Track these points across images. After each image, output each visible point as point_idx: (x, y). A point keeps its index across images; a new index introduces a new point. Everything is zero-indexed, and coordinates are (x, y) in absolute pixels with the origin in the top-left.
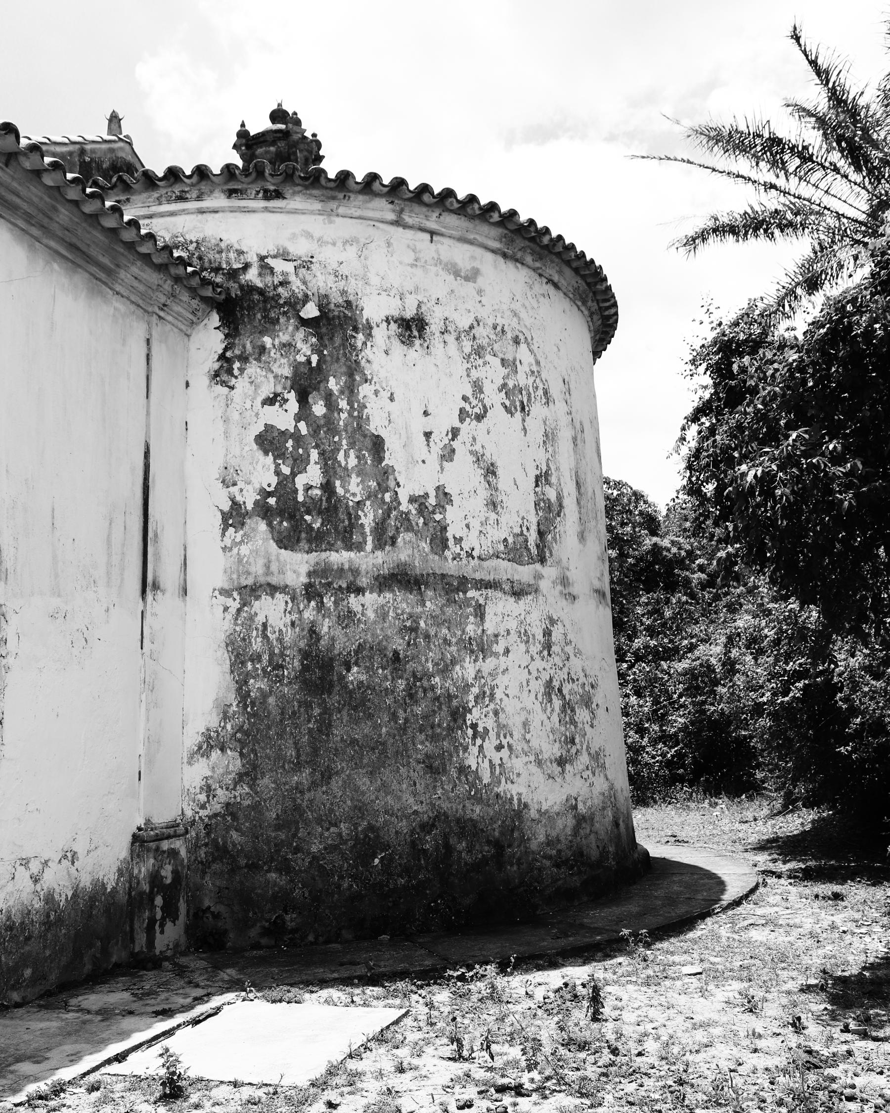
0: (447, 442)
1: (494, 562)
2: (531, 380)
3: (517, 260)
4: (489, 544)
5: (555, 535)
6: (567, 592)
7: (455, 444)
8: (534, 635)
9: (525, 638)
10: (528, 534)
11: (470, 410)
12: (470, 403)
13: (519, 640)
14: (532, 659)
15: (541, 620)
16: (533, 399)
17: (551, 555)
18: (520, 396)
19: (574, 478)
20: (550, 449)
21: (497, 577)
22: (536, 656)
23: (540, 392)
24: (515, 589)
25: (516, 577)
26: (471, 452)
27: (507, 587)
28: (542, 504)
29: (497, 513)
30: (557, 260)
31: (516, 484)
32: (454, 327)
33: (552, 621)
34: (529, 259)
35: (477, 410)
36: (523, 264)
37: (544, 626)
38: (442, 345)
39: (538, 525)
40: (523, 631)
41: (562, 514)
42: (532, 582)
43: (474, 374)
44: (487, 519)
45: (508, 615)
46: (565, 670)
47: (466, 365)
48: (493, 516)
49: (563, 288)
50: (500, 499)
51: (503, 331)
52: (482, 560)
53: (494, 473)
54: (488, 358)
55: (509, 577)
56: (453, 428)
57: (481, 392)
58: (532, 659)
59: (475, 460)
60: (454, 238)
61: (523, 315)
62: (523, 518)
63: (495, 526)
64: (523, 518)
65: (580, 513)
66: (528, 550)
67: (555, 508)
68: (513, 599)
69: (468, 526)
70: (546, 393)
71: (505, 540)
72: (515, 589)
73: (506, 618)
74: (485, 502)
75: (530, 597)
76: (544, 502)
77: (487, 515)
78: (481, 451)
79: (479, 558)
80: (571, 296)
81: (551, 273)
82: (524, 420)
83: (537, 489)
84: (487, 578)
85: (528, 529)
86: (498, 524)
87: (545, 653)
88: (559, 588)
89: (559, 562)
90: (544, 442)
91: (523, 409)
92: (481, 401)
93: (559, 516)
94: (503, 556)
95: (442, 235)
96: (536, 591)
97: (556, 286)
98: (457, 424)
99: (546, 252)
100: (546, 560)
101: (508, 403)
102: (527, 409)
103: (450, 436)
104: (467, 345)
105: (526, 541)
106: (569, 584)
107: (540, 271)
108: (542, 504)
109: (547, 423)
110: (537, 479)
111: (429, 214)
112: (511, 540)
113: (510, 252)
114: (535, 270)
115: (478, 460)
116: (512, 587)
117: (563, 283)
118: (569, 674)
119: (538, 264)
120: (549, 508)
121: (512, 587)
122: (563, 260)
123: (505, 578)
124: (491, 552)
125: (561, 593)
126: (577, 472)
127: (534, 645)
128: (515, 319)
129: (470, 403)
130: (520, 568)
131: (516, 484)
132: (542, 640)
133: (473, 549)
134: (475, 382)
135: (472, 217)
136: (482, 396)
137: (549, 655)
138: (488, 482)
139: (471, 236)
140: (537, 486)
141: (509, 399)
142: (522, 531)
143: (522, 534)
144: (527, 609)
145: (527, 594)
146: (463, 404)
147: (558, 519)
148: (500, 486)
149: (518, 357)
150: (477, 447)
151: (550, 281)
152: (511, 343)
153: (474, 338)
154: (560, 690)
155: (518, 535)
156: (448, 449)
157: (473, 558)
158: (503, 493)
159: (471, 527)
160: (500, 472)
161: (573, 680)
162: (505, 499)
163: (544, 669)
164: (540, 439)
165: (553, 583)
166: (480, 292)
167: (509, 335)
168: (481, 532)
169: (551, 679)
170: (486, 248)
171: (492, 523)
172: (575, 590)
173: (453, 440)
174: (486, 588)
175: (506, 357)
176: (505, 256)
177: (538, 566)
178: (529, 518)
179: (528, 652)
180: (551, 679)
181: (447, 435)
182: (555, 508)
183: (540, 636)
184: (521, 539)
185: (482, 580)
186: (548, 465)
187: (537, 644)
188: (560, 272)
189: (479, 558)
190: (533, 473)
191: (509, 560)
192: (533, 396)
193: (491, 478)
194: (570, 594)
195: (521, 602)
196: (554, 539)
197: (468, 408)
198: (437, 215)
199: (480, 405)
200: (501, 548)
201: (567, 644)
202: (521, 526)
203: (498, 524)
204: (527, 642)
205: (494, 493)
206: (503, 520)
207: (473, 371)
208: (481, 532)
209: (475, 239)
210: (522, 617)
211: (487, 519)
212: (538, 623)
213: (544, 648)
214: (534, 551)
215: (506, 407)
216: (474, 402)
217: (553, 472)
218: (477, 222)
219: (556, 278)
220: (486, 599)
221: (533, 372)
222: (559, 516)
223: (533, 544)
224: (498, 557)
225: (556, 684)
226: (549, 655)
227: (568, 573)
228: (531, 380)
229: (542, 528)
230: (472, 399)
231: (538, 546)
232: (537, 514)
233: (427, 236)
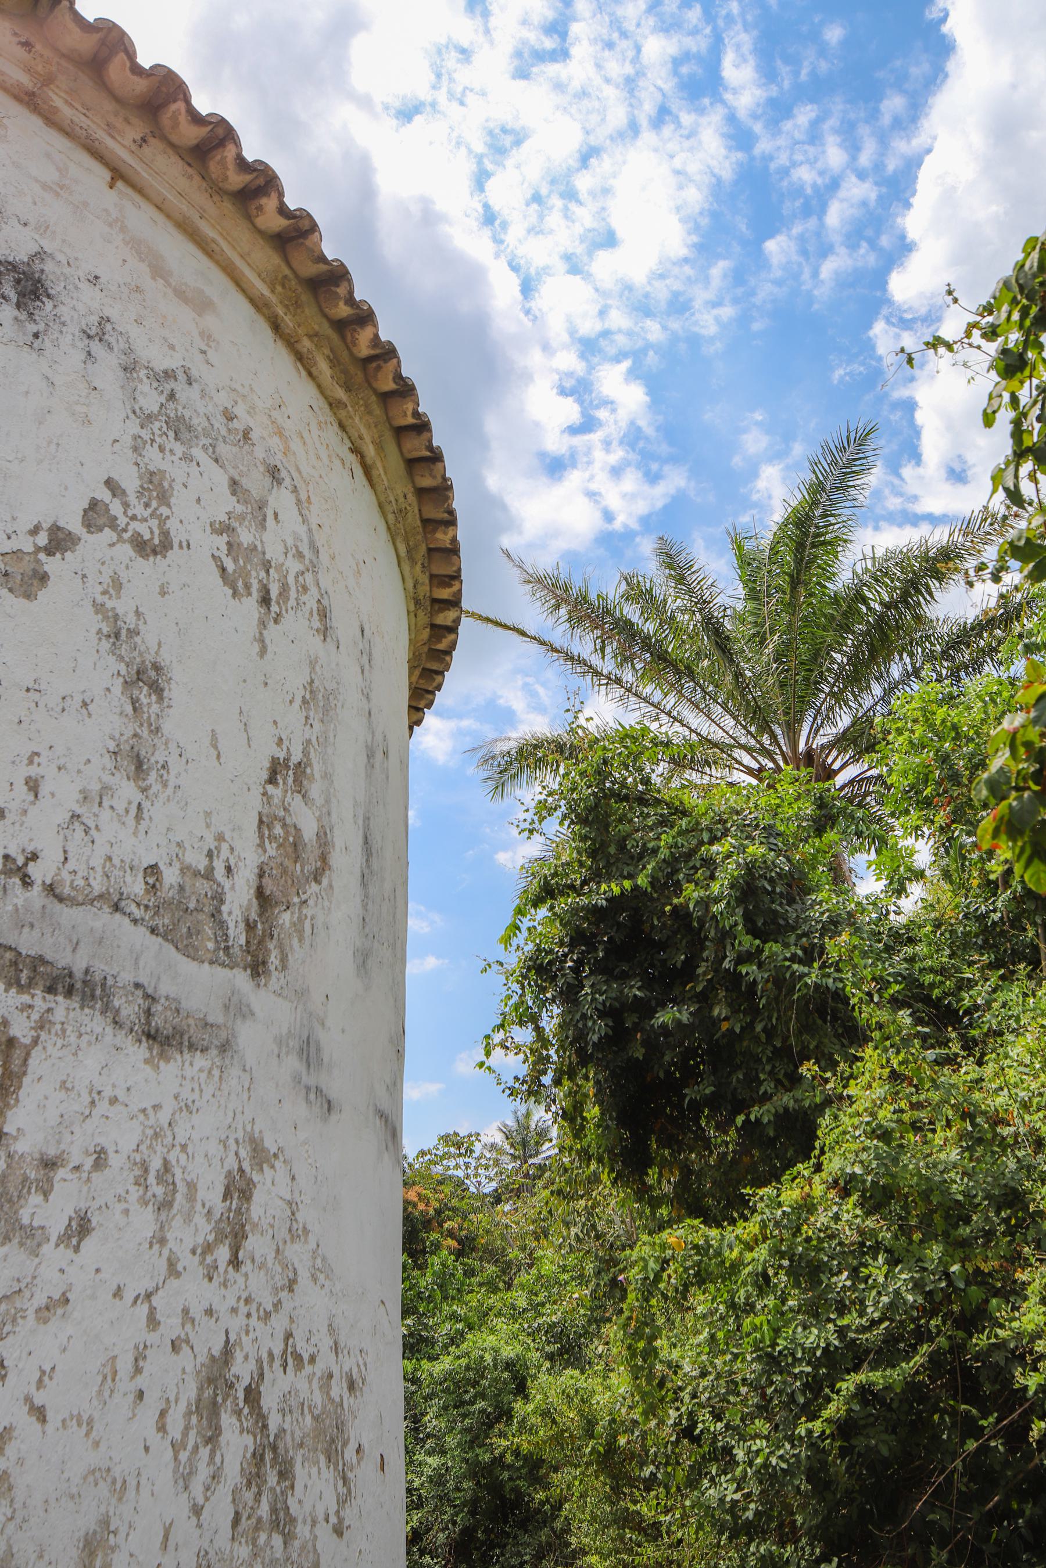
0: (29, 548)
1: (102, 919)
2: (294, 566)
3: (299, 357)
4: (97, 862)
5: (301, 920)
6: (312, 1081)
7: (51, 565)
8: (192, 1186)
9: (159, 1190)
10: (227, 884)
11: (122, 521)
12: (126, 505)
13: (135, 1193)
14: (173, 1269)
15: (224, 1142)
16: (292, 603)
17: (284, 966)
18: (263, 574)
19: (360, 822)
20: (317, 725)
21: (100, 968)
22: (187, 1261)
23: (310, 600)
24: (157, 1021)
25: (166, 988)
26: (99, 608)
27: (129, 1009)
28: (278, 830)
29: (144, 790)
30: (378, 411)
31: (216, 747)
32: (122, 345)
33: (261, 1156)
34: (323, 367)
35: (143, 529)
36: (310, 374)
37: (231, 1163)
38: (83, 356)
39: (261, 876)
40: (156, 1164)
41: (325, 881)
42: (216, 1017)
43: (153, 457)
44: (105, 790)
45: (113, 1101)
46: (279, 1323)
47: (133, 427)
48: (127, 791)
49: (380, 488)
50: (160, 757)
51: (246, 435)
52: (61, 899)
53: (157, 689)
54: (197, 452)
55: (143, 980)
56: (55, 529)
57: (164, 498)
58: (173, 1269)
59: (105, 630)
60: (168, 216)
61: (296, 445)
62: (220, 838)
63: (130, 820)
64: (220, 838)
65: (365, 907)
66: (222, 925)
67: (312, 863)
68: (138, 1052)
69: (33, 786)
70: (323, 614)
71: (153, 870)
72: (157, 1021)
73: (103, 1107)
74: (112, 745)
75: (201, 1061)
76: (284, 826)
77: (107, 778)
78: (131, 620)
79: (50, 889)
80: (391, 517)
81: (364, 431)
82: (263, 624)
83: (270, 788)
84: (63, 959)
85: (229, 869)
86: (139, 817)
87: (223, 1253)
88: (293, 1063)
89: (302, 994)
90: (305, 701)
91: (265, 600)
92: (163, 521)
93: (318, 881)
94: (138, 913)
95: (140, 190)
96: (224, 1048)
97: (367, 470)
98: (74, 524)
99: (360, 376)
100: (267, 973)
101: (230, 566)
102: (274, 608)
103: (42, 539)
104: (151, 400)
105: (219, 898)
106: (320, 1062)
107: (342, 413)
108: (278, 830)
109: (317, 668)
110: (275, 771)
111: (119, 123)
112: (171, 876)
113: (288, 321)
114: (334, 405)
115: (117, 635)
116: (148, 1013)
117: (379, 471)
118: (289, 1336)
119: (340, 394)
120: (295, 847)
121: (148, 1013)
122: (388, 419)
123: (127, 977)
124: (98, 886)
125: (297, 1080)
126: (367, 819)
127: (188, 1219)
128: (276, 439)
129: (126, 505)
130: (186, 966)
131: (216, 747)
132: (220, 1208)
133: (34, 857)
134: (152, 474)
135: (217, 189)
136: (164, 511)
137: (235, 1262)
138: (134, 702)
139: (208, 231)
140: (272, 780)
141: (235, 560)
142: (210, 869)
143: (208, 875)
144: (185, 1094)
145: (191, 1047)
146: (104, 495)
147: (314, 887)
148: (168, 727)
149: (271, 500)
150: (123, 606)
151: (355, 450)
152: (262, 469)
153: (172, 396)
154: (252, 1395)
155: (197, 874)
156: (26, 565)
157: (27, 882)
158: (172, 746)
159: (44, 790)
160: (175, 692)
161: (298, 1358)
162: (175, 765)
163: (209, 1312)
164: (297, 682)
165: (279, 1041)
166: (207, 336)
167: (259, 453)
168: (75, 817)
169: (227, 1352)
170: (238, 282)
171: (120, 807)
172: (336, 1086)
173: (50, 551)
174: (51, 990)
175: (244, 481)
176: (276, 327)
177: (241, 978)
178: (238, 845)
179: (163, 1241)
180: (227, 1352)
181: (35, 531)
182: (311, 855)
183: (212, 1194)
184: (203, 886)
185: (41, 960)
186: (306, 753)
187: (199, 1220)
188: (379, 446)
189: (50, 889)
190: (266, 751)
191: (153, 931)
192: (293, 594)
193: (143, 694)
194: (319, 1090)
195: (170, 1069)
196: (298, 927)
197: (116, 508)
198: (138, 137)
199: (154, 523)
200: (137, 887)
201: (294, 1236)
202: (210, 854)
203: (139, 817)
204: (165, 1205)
205: (145, 733)
206: (157, 812)
207: (152, 453)
208: (75, 817)
209: (214, 241)
210: (164, 1117)
211: (105, 790)
212: (214, 1148)
213: (220, 1237)
214: (238, 935)
215: (223, 570)
216: (139, 510)
217: (317, 776)
218: (228, 206)
219: (370, 451)
220: (42, 1024)
221: (300, 555)
222: (318, 881)
223: (237, 914)
224: (116, 908)
225: (242, 1370)
226: (235, 1262)
227: (321, 1035)
228: (294, 566)
229: (269, 887)
230: (132, 498)
231: (250, 927)
232: (261, 845)
233: (107, 175)
